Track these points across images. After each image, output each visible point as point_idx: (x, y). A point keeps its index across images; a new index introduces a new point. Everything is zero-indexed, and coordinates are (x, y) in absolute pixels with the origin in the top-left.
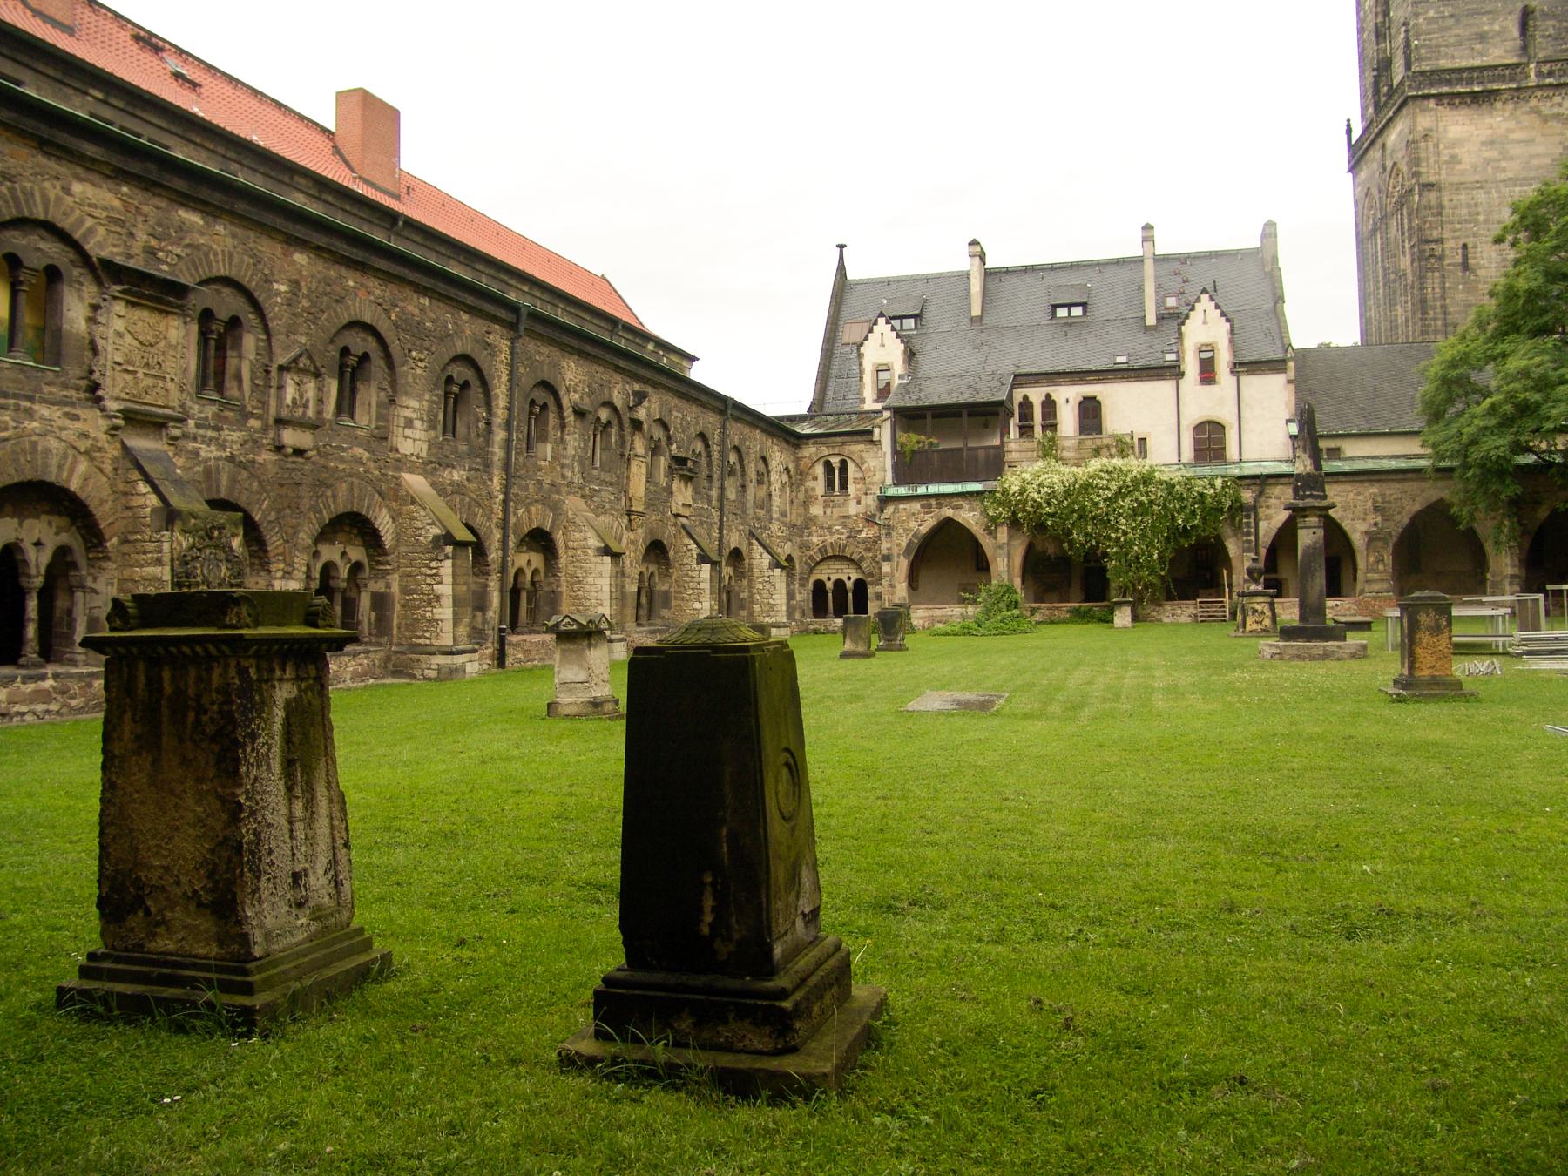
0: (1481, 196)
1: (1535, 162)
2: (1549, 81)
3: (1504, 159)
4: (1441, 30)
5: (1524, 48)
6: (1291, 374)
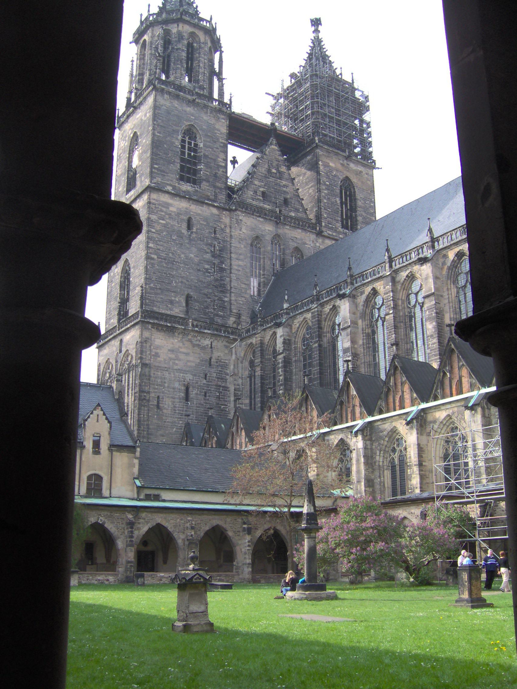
0: (167, 375)
1: (189, 364)
2: (196, 329)
3: (177, 359)
4: (156, 294)
5: (187, 312)
6: (138, 454)
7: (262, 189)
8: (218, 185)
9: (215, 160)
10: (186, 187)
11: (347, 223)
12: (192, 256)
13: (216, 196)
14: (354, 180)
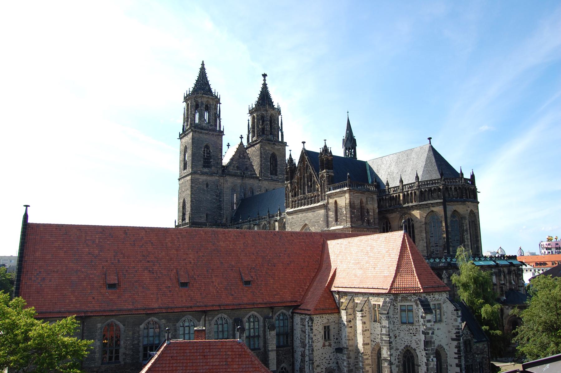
5: (207, 220)
7: (236, 165)
8: (218, 166)
9: (217, 156)
10: (206, 170)
11: (273, 172)
12: (208, 197)
13: (218, 172)
14: (277, 153)
